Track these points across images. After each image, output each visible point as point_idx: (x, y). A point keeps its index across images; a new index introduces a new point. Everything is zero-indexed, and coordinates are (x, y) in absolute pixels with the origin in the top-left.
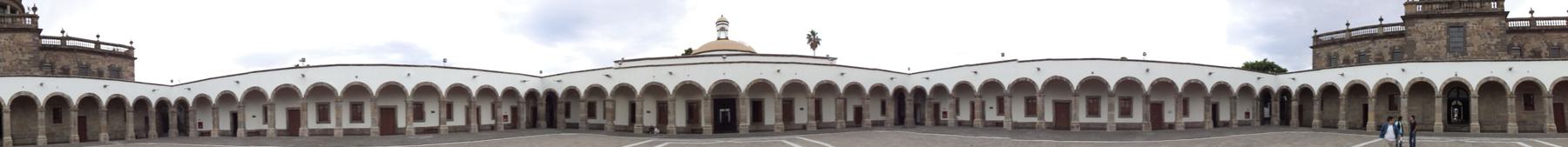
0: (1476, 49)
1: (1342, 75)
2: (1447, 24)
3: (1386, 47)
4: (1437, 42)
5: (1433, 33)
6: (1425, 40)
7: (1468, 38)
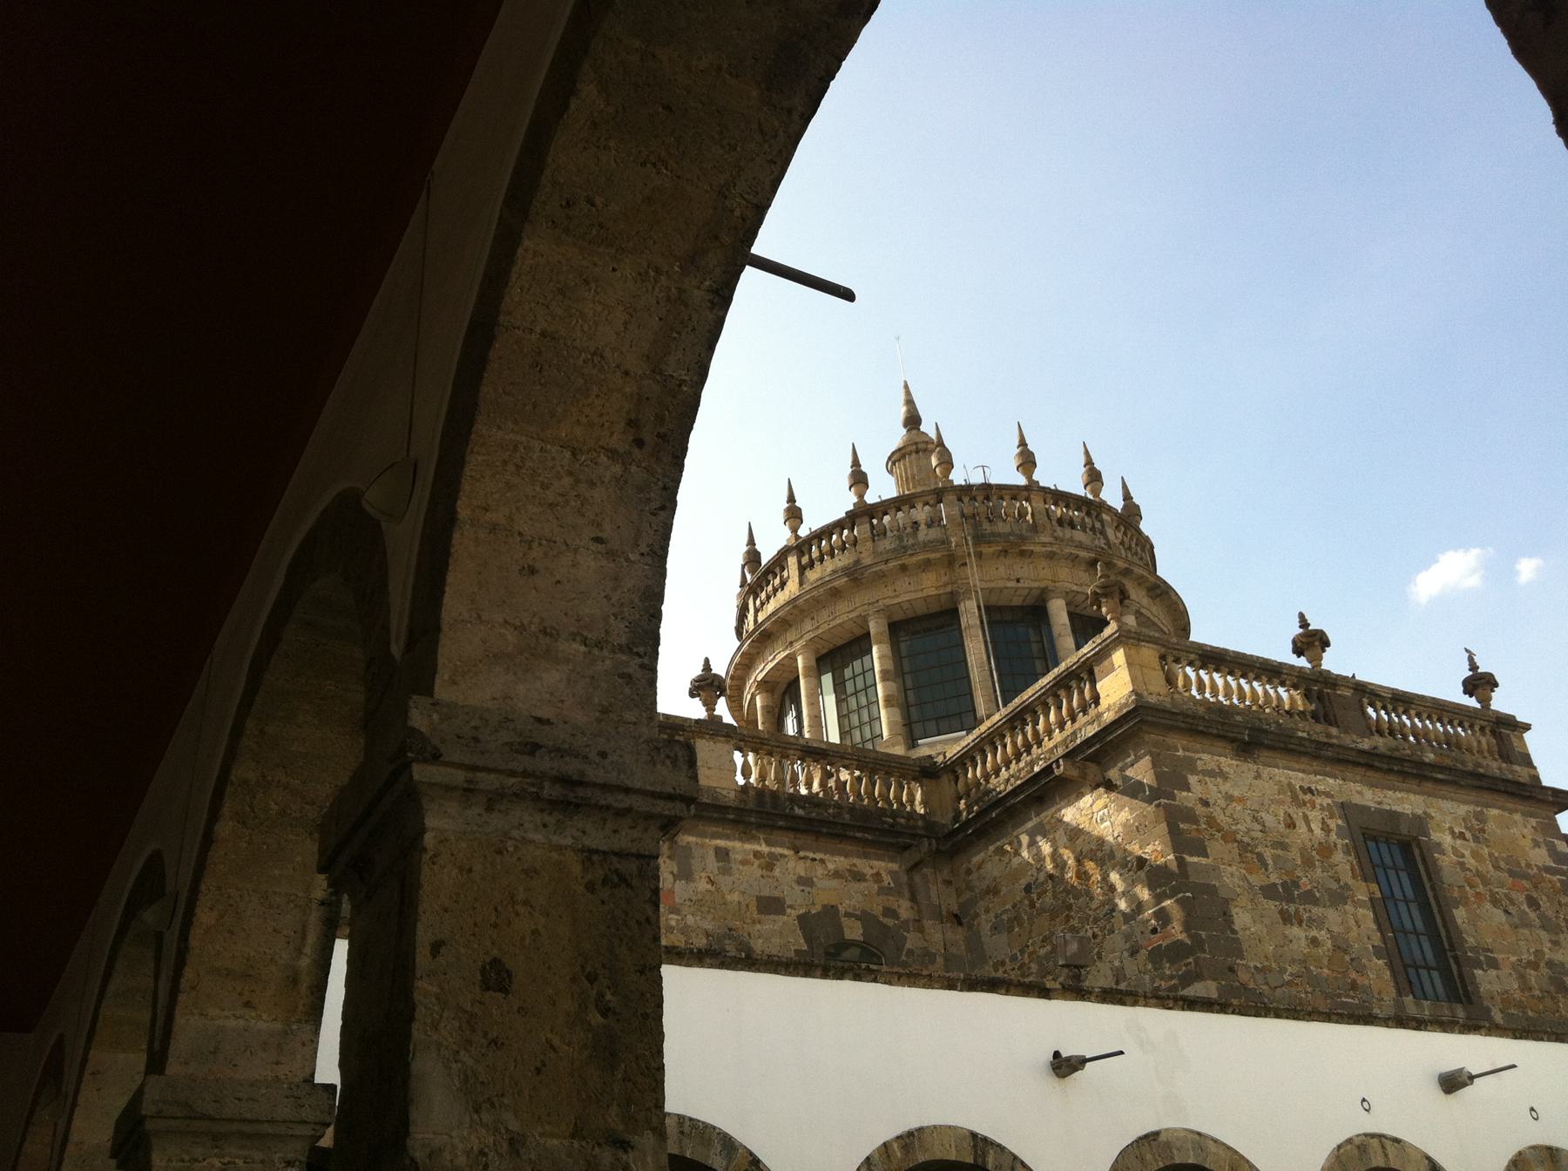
5: (1294, 854)
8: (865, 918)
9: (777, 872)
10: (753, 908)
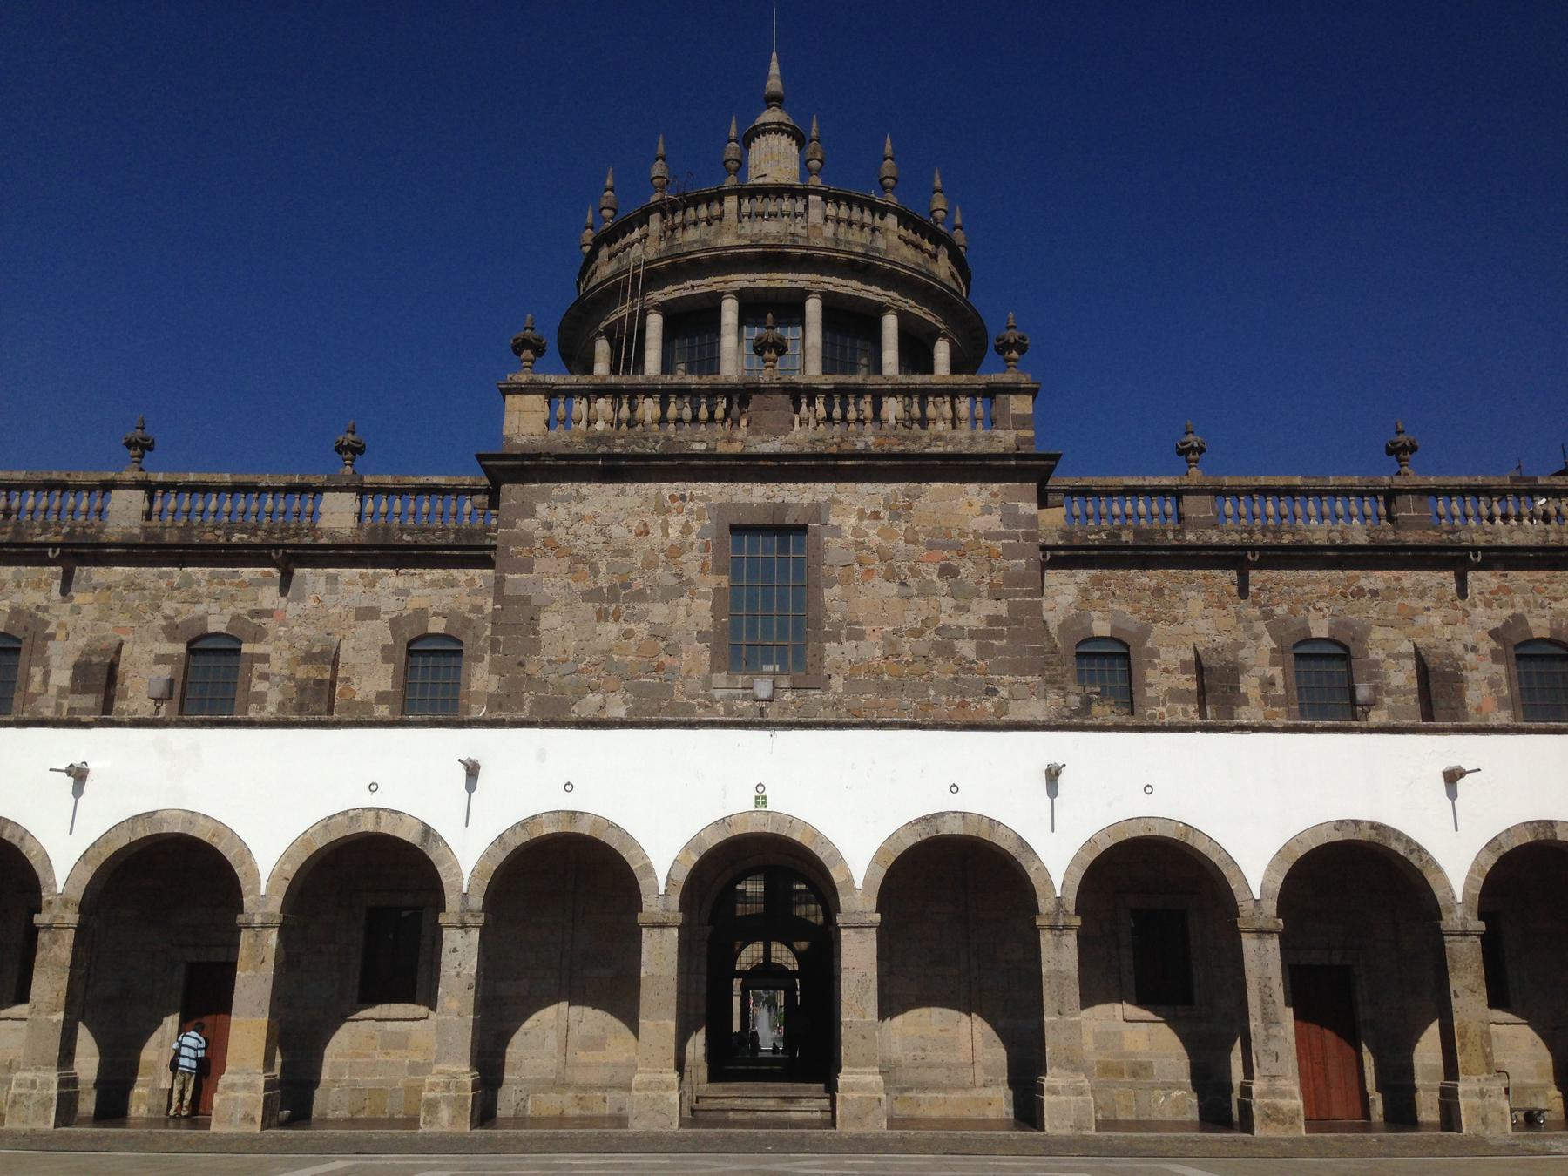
0: (872, 650)
2: (722, 508)
3: (367, 614)
5: (638, 559)
6: (588, 596)
7: (830, 595)
8: (449, 615)
9: (377, 588)
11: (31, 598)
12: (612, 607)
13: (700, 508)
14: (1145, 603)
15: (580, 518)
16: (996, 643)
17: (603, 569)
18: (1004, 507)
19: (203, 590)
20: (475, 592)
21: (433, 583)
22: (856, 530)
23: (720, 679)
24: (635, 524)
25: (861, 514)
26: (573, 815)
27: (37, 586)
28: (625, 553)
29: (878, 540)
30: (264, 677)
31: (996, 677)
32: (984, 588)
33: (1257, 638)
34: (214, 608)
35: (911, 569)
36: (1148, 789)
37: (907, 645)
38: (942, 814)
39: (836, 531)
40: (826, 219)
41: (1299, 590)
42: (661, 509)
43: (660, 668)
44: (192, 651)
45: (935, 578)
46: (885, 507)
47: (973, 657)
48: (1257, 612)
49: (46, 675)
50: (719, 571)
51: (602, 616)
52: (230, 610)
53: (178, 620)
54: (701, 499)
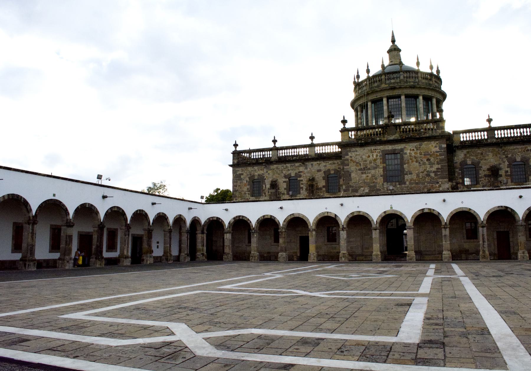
0: (414, 176)
1: (281, 208)
3: (319, 171)
4: (373, 172)
5: (368, 162)
6: (360, 170)
7: (405, 166)
8: (335, 170)
9: (320, 165)
10: (316, 171)
11: (261, 172)
12: (364, 171)
13: (379, 151)
14: (479, 157)
15: (357, 155)
16: (438, 173)
17: (362, 164)
18: (439, 146)
19: (289, 168)
20: (339, 165)
21: (331, 164)
22: (410, 153)
23: (385, 184)
24: (367, 155)
25: (411, 150)
26: (359, 212)
27: (262, 170)
28: (366, 161)
29: (414, 155)
30: (302, 184)
31: (439, 180)
32: (436, 163)
33: (504, 162)
34: (292, 172)
35: (421, 160)
36: (462, 202)
37: (421, 175)
38: (424, 209)
39: (406, 154)
40: (404, 77)
41: (514, 151)
42: (372, 152)
43: (374, 182)
44: (289, 180)
45: (426, 161)
46: (415, 148)
47: (434, 176)
48: (504, 156)
49: (266, 186)
50: (383, 163)
51: (362, 173)
52: (295, 172)
53: (286, 174)
54: (379, 149)
